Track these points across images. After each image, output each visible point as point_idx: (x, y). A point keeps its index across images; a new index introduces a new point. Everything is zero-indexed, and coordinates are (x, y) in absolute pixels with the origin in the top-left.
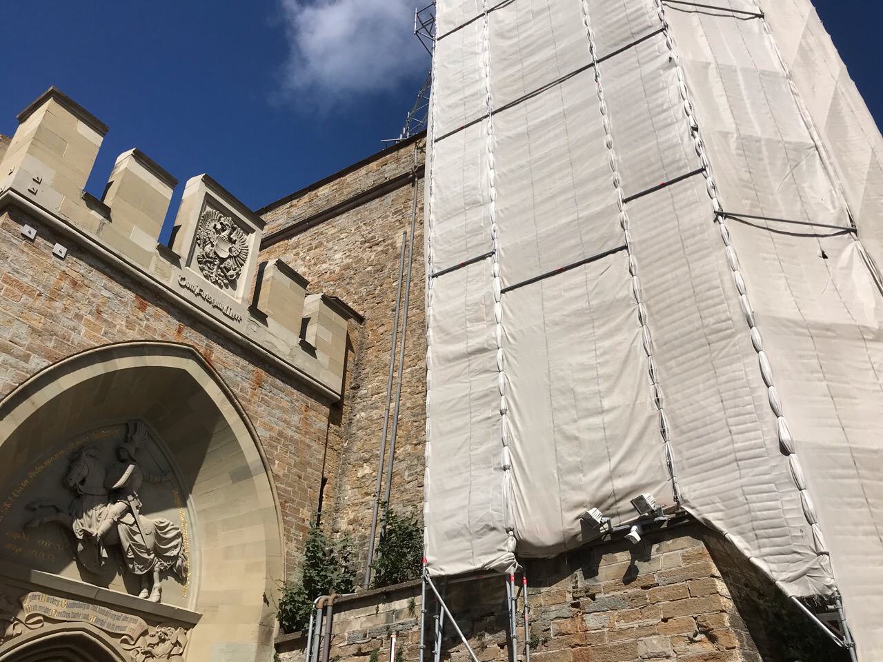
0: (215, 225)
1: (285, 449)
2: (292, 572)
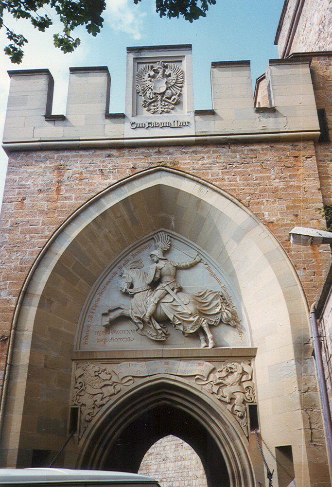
0: (149, 75)
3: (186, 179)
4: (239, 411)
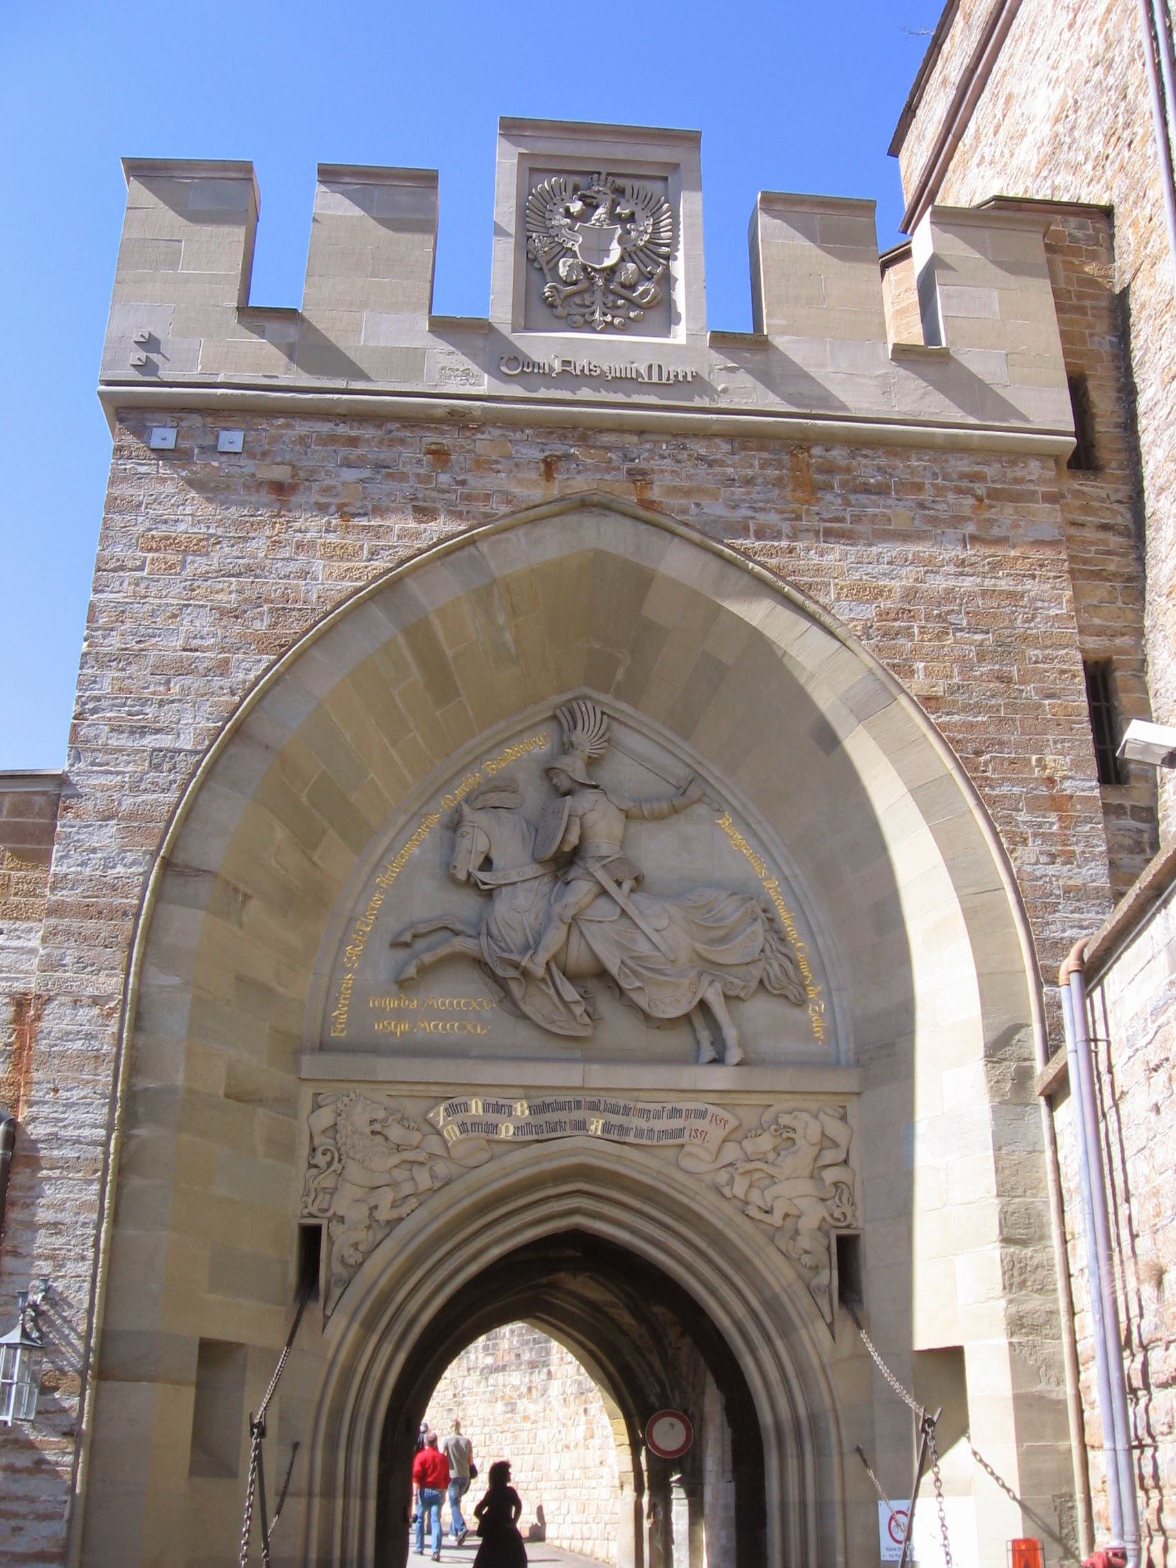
1: (936, 627)
2: (1050, 918)
3: (676, 540)
4: (806, 1252)
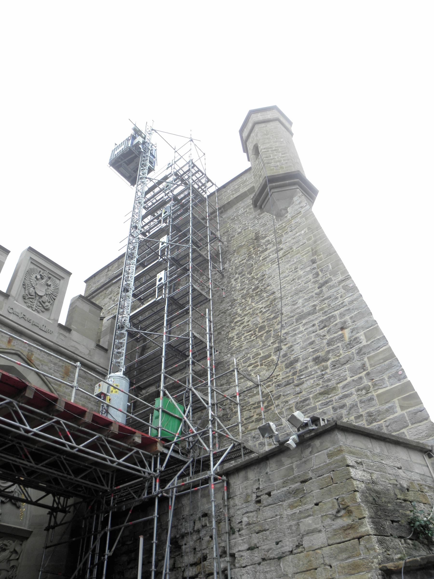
0: (36, 276)
